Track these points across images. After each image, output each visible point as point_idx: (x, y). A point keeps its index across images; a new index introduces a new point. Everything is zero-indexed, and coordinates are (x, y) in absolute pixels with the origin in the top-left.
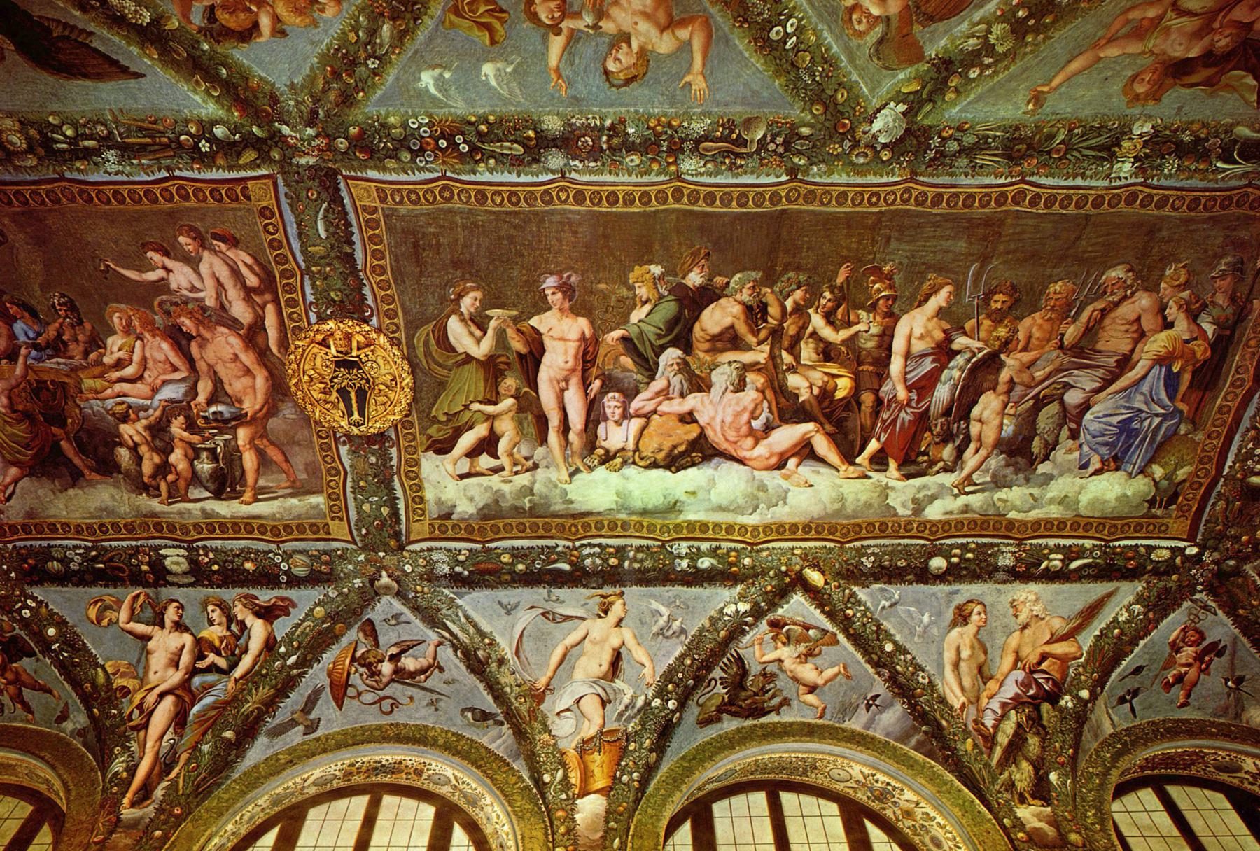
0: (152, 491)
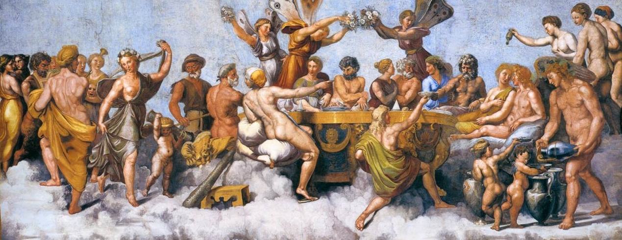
0: (487, 218)
